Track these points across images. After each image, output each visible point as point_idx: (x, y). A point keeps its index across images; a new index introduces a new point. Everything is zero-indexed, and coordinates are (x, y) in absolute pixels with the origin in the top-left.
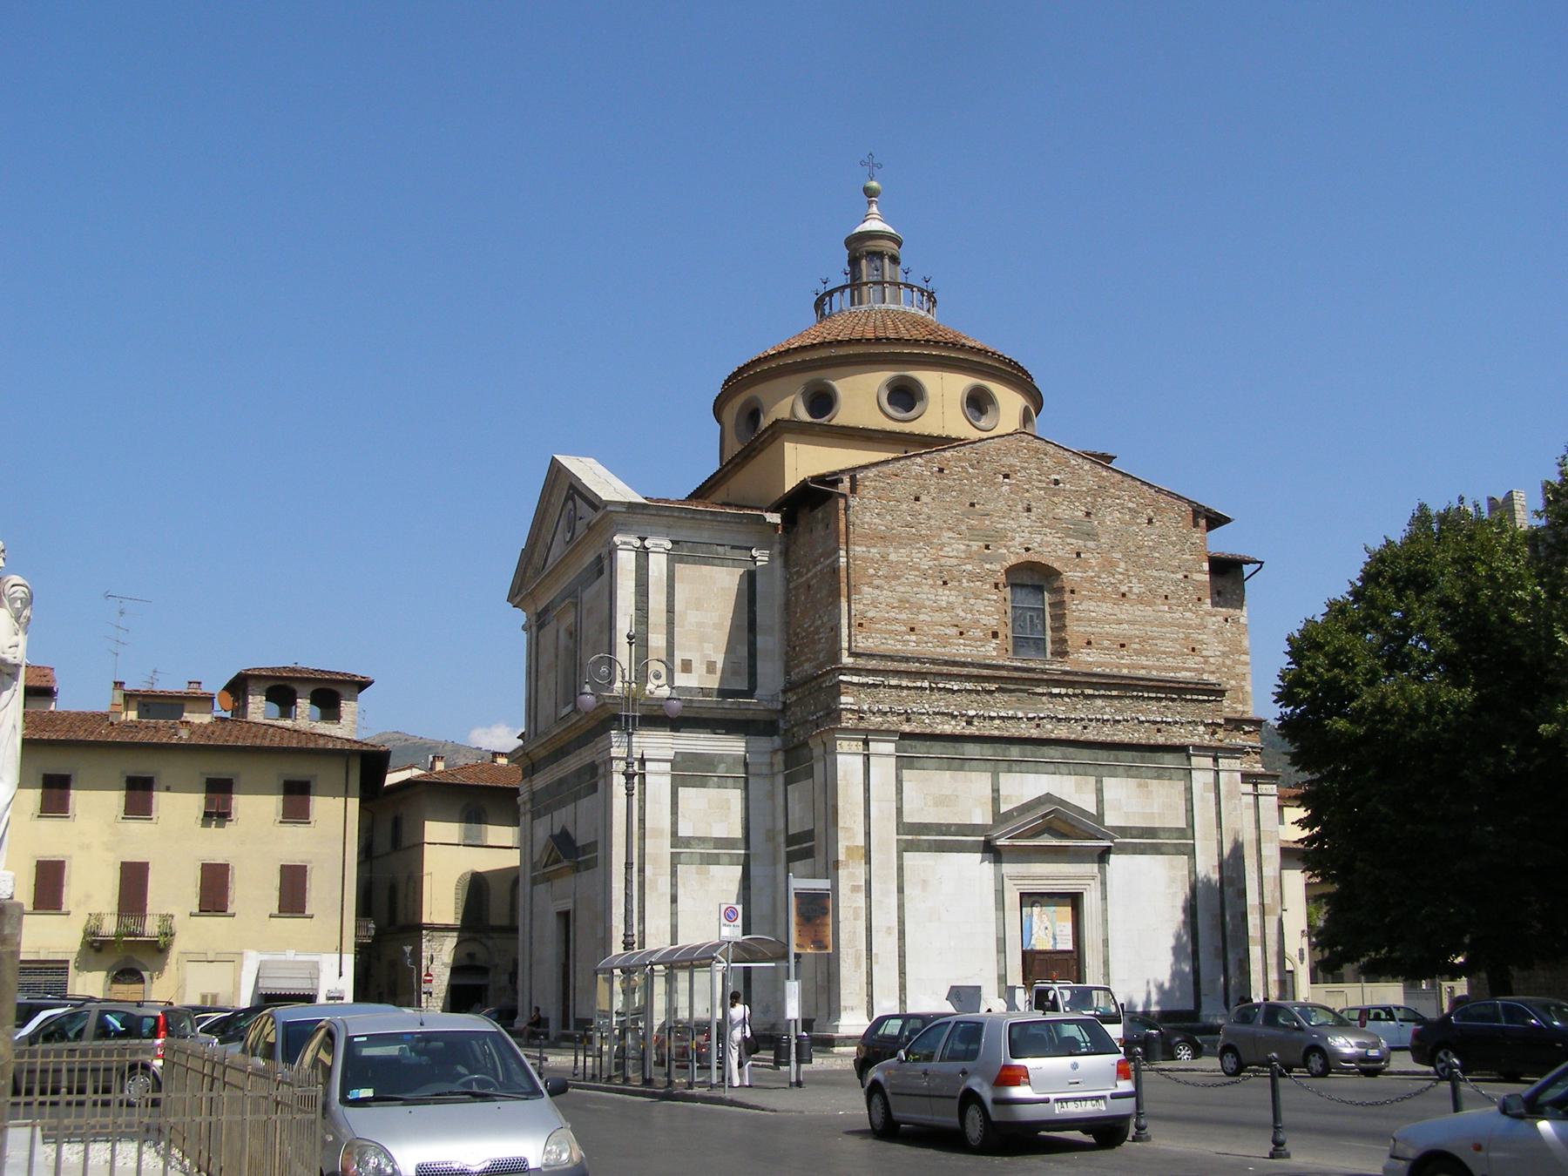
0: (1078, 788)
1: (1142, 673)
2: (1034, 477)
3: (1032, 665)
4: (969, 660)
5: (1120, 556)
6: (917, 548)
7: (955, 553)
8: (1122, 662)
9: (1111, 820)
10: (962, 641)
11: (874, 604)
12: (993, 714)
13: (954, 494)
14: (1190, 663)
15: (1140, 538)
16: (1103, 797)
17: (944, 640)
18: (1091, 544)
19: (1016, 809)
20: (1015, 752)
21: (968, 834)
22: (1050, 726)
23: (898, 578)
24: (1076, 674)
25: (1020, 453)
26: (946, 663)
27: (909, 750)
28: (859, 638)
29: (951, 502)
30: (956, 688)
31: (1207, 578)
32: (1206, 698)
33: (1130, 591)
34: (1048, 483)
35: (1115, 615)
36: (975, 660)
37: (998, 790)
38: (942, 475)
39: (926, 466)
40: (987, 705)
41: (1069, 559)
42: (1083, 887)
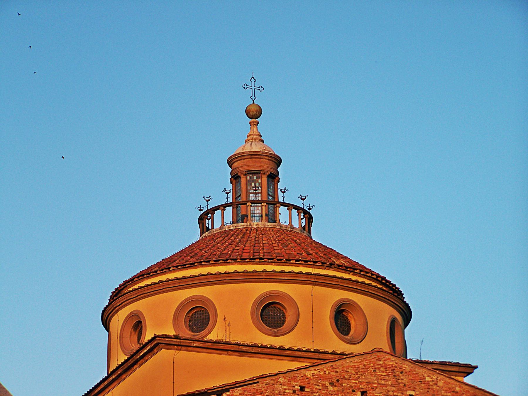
39: (289, 385)
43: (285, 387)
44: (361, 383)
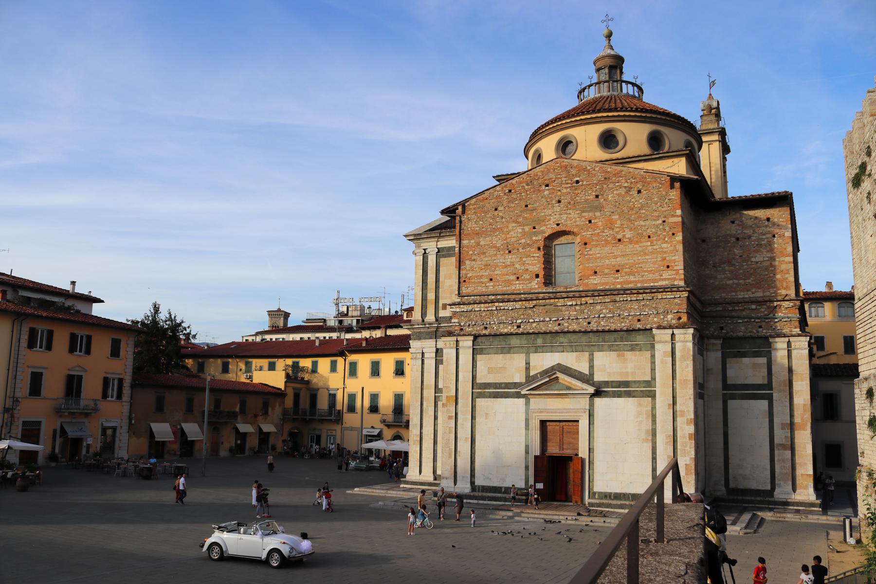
0: (578, 360)
2: (564, 182)
3: (559, 290)
4: (522, 292)
5: (617, 217)
6: (495, 236)
7: (515, 235)
8: (618, 281)
9: (597, 378)
10: (517, 282)
11: (472, 269)
12: (531, 321)
13: (517, 202)
15: (632, 203)
16: (593, 363)
17: (508, 283)
18: (598, 214)
19: (540, 373)
20: (539, 341)
21: (512, 387)
22: (566, 324)
23: (484, 253)
25: (556, 170)
26: (508, 294)
27: (481, 344)
28: (463, 288)
29: (514, 206)
30: (510, 308)
31: (680, 219)
32: (673, 297)
33: (624, 236)
34: (572, 184)
35: (613, 253)
36: (526, 291)
37: (529, 363)
38: (511, 193)
39: (502, 191)
41: (584, 225)
42: (579, 417)
43: (500, 192)
44: (545, 180)
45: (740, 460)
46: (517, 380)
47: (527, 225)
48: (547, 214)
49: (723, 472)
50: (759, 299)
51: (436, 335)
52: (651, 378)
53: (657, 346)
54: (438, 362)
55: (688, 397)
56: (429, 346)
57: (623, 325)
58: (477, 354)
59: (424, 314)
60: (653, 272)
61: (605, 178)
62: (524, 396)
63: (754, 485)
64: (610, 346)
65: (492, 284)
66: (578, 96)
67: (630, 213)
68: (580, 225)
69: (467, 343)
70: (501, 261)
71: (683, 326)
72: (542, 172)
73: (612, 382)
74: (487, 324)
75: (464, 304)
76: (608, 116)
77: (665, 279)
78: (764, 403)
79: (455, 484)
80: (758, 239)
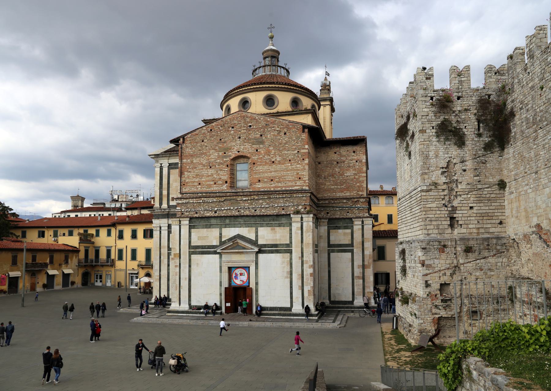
1: (279, 189)
2: (242, 126)
3: (238, 191)
5: (272, 148)
7: (214, 157)
8: (272, 186)
9: (260, 242)
10: (215, 186)
11: (188, 177)
12: (222, 209)
13: (215, 137)
14: (298, 183)
17: (209, 186)
18: (261, 146)
19: (228, 240)
20: (227, 221)
22: (243, 211)
23: (195, 168)
24: (254, 192)
26: (210, 193)
28: (183, 189)
30: (211, 201)
33: (276, 159)
37: (221, 234)
39: (207, 130)
40: (222, 206)
41: (253, 152)
44: (232, 124)
45: (337, 285)
46: (214, 244)
47: (221, 152)
48: (232, 145)
49: (328, 292)
50: (348, 197)
51: (168, 215)
52: (290, 242)
53: (293, 224)
54: (169, 232)
55: (310, 253)
56: (164, 222)
57: (274, 211)
58: (191, 228)
59: (161, 204)
60: (291, 181)
61: (266, 125)
62: (219, 253)
63: (344, 299)
64: (267, 224)
65: (200, 186)
66: (253, 74)
67: (280, 146)
68: (251, 152)
69: (185, 222)
70: (206, 172)
71: (308, 213)
72: (230, 119)
73: (268, 244)
74: (197, 211)
75: (184, 199)
76: (269, 87)
77: (298, 186)
78: (350, 254)
79: (180, 304)
80: (349, 163)
